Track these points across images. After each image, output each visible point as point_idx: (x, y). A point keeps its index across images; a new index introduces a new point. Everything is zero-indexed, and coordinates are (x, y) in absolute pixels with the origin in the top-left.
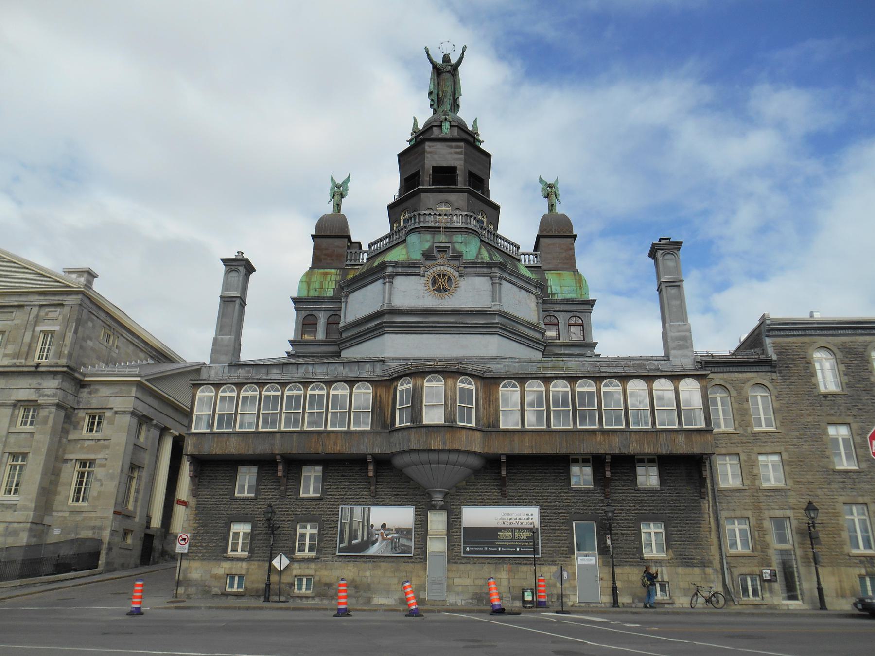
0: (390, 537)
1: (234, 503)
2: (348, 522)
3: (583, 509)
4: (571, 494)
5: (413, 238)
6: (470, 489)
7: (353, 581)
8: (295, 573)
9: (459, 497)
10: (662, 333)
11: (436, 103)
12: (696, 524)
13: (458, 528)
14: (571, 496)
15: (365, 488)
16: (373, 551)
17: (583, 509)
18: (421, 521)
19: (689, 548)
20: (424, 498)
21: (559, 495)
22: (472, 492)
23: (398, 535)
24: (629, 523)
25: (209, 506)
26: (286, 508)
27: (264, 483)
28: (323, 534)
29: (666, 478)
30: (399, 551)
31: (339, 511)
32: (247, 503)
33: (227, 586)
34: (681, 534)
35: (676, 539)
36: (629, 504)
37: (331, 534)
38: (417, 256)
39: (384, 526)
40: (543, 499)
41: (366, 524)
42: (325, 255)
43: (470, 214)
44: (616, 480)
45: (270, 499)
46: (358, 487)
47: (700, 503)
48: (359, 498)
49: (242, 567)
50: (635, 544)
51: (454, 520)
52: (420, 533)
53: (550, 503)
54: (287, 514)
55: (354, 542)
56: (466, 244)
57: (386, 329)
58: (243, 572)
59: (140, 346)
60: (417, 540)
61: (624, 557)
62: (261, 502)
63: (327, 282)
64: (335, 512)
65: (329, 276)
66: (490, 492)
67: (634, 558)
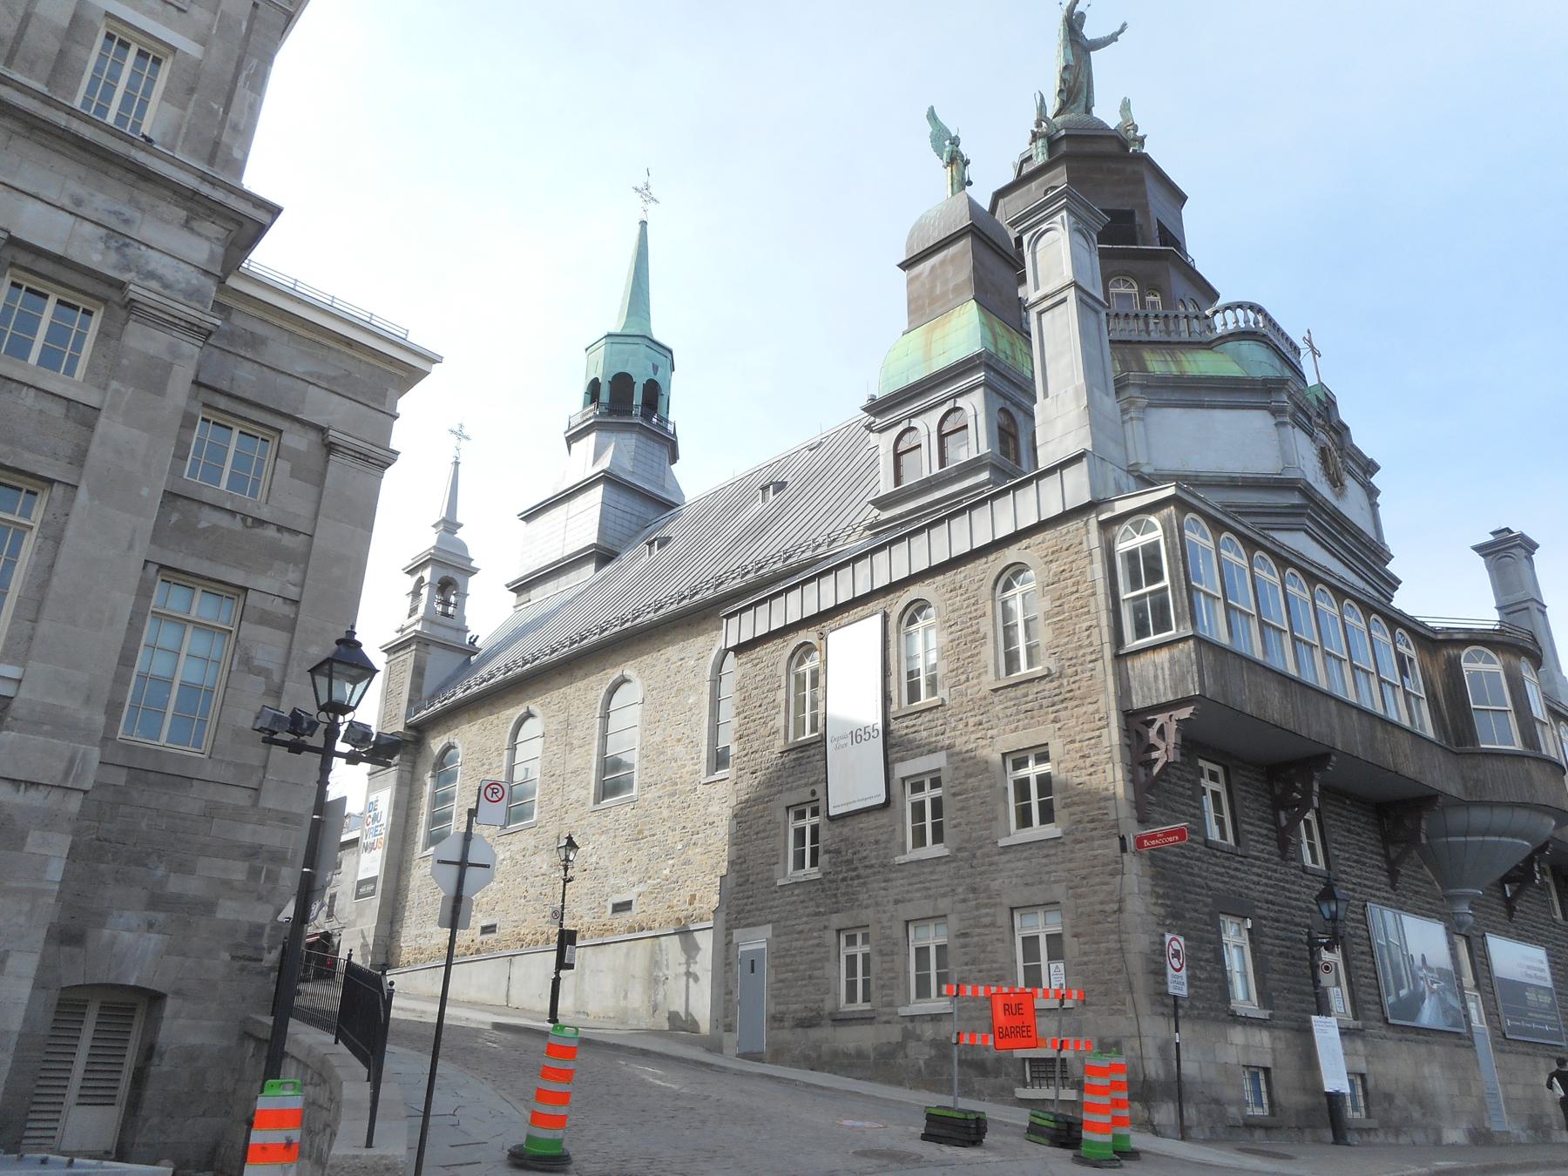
0: (1435, 986)
16: (1428, 1015)
23: (1442, 984)
25: (1174, 859)
27: (1248, 817)
30: (1450, 1021)
48: (1378, 889)
55: (1403, 993)
62: (1253, 865)
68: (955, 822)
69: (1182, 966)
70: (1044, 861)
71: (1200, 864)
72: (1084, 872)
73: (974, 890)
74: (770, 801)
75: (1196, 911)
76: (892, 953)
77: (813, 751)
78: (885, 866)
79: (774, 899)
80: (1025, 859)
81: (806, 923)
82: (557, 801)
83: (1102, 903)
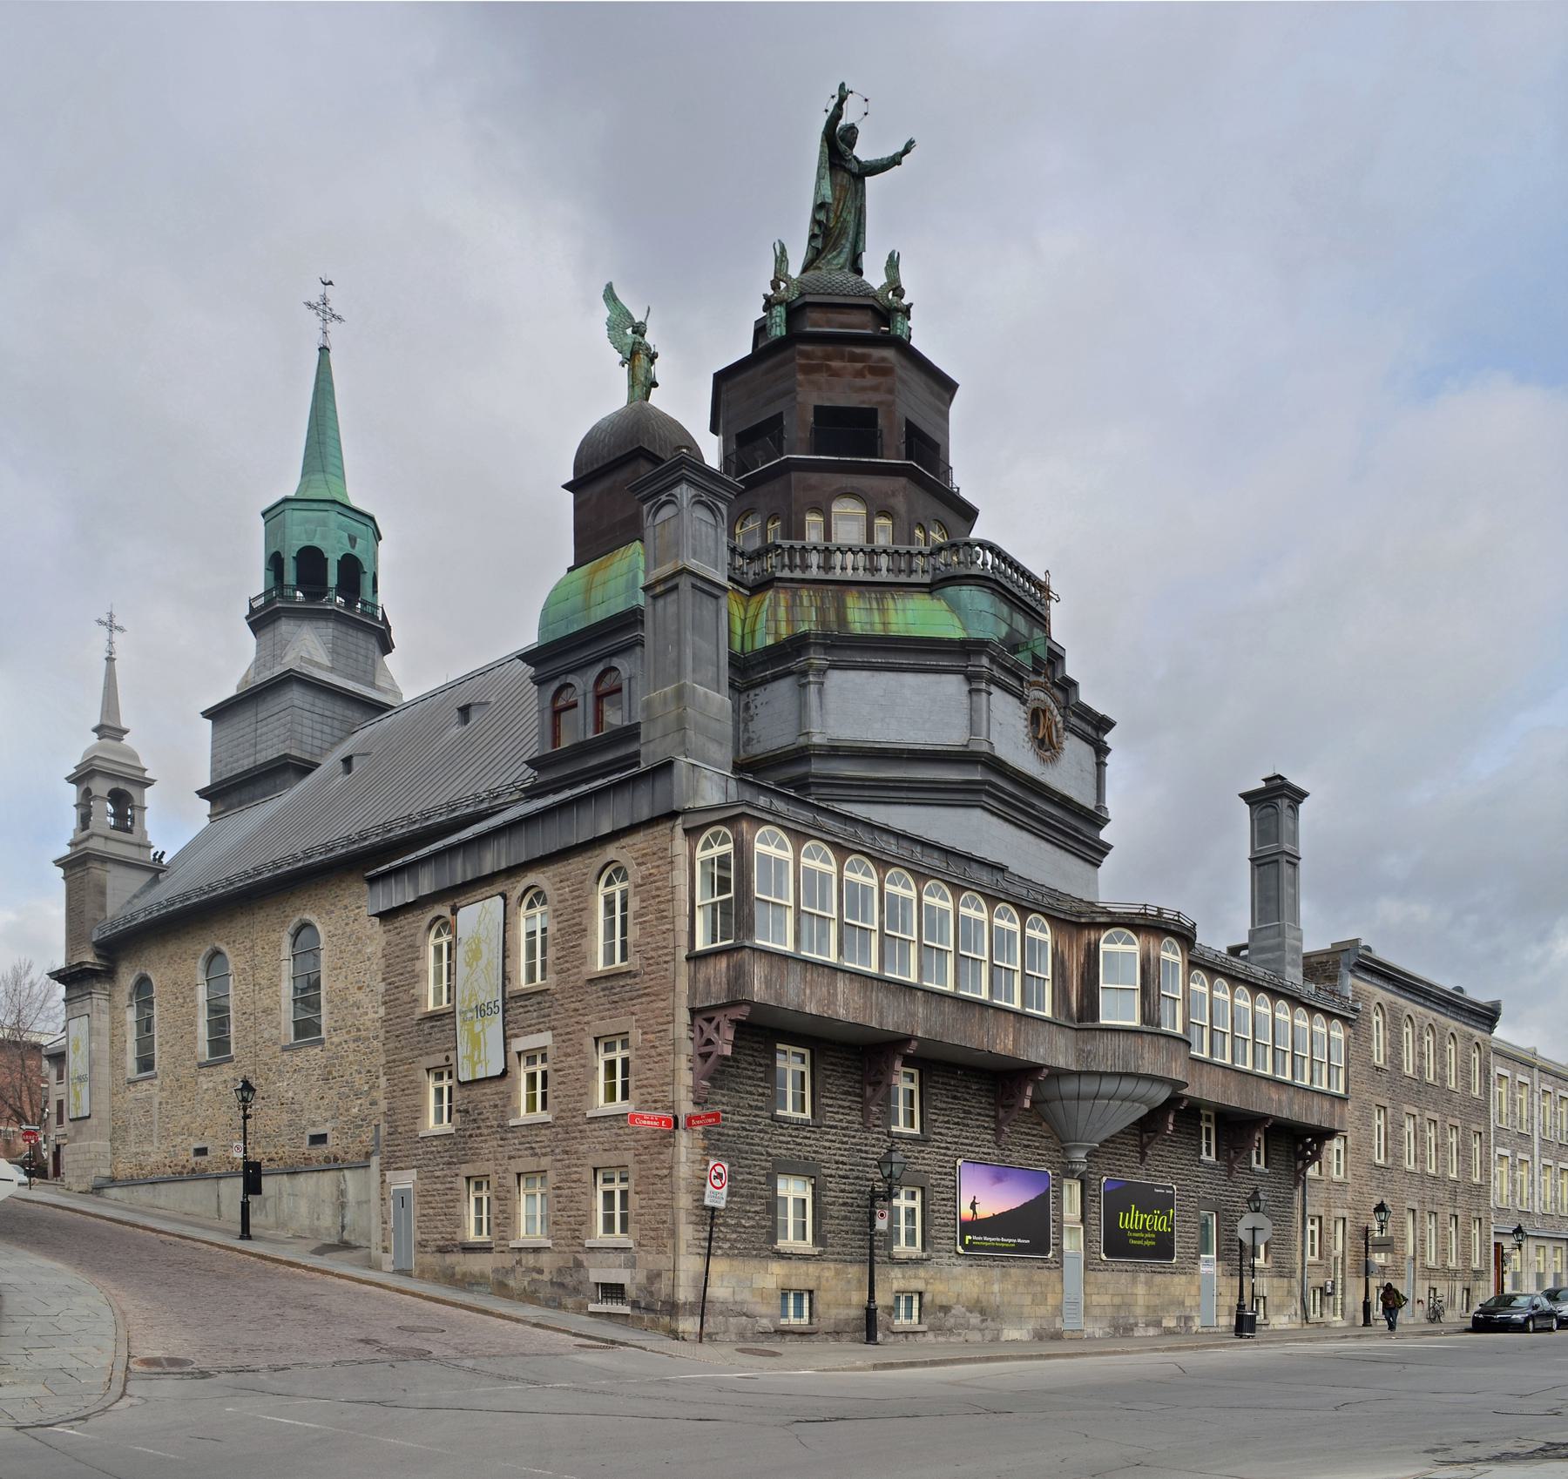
1: (780, 1131)
7: (978, 1301)
8: (896, 1286)
15: (986, 1128)
20: (1058, 1157)
25: (731, 1132)
28: (933, 1211)
32: (805, 1134)
37: (945, 1212)
46: (978, 1123)
48: (979, 1146)
49: (808, 1275)
68: (555, 1094)
70: (619, 1131)
71: (762, 1135)
72: (646, 1143)
73: (566, 1152)
74: (413, 1062)
75: (750, 1174)
76: (506, 1199)
77: (447, 1021)
78: (502, 1127)
79: (417, 1148)
80: (606, 1129)
81: (443, 1169)
82: (251, 1037)
83: (657, 1169)
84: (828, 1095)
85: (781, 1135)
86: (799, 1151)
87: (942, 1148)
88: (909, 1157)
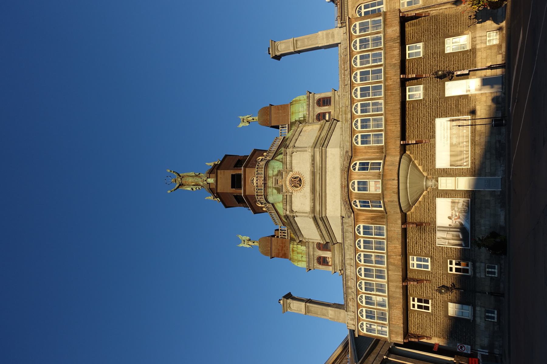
1: (435, 313)
2: (447, 240)
3: (437, 91)
4: (427, 99)
5: (271, 199)
6: (424, 163)
8: (483, 276)
9: (430, 170)
10: (325, 49)
11: (198, 187)
12: (446, 18)
13: (451, 170)
14: (428, 99)
15: (424, 229)
17: (437, 91)
18: (446, 194)
19: (463, 20)
21: (427, 106)
22: (426, 162)
23: (456, 208)
24: (446, 60)
25: (438, 329)
26: (438, 280)
29: (416, 40)
31: (440, 246)
32: (435, 305)
33: (493, 320)
34: (454, 26)
35: (457, 29)
36: (434, 61)
37: (456, 252)
38: (280, 197)
39: (450, 218)
40: (431, 117)
41: (448, 229)
42: (282, 251)
43: (257, 167)
44: (417, 71)
45: (432, 290)
47: (432, 16)
48: (431, 233)
50: (460, 56)
51: (446, 173)
52: (454, 195)
53: (433, 111)
54: (443, 279)
55: (461, 237)
56: (274, 168)
57: (323, 215)
58: (483, 309)
59: (339, 362)
60: (459, 197)
61: (469, 62)
62: (434, 296)
63: (298, 250)
64: (441, 249)
65: (294, 249)
66: (426, 150)
67: (471, 55)
69: (464, 346)
84: (423, 294)
85: (437, 313)
86: (441, 307)
87: (434, 250)
88: (438, 265)
